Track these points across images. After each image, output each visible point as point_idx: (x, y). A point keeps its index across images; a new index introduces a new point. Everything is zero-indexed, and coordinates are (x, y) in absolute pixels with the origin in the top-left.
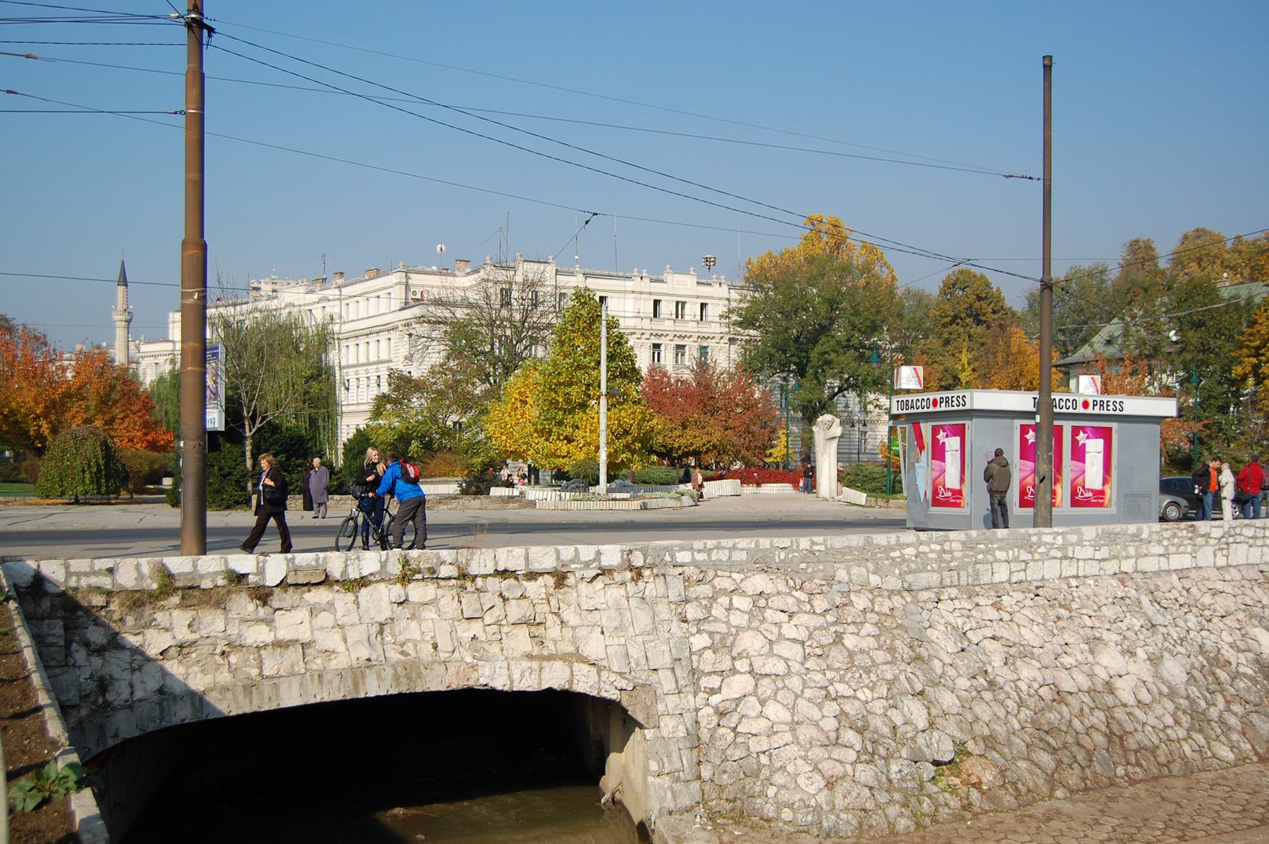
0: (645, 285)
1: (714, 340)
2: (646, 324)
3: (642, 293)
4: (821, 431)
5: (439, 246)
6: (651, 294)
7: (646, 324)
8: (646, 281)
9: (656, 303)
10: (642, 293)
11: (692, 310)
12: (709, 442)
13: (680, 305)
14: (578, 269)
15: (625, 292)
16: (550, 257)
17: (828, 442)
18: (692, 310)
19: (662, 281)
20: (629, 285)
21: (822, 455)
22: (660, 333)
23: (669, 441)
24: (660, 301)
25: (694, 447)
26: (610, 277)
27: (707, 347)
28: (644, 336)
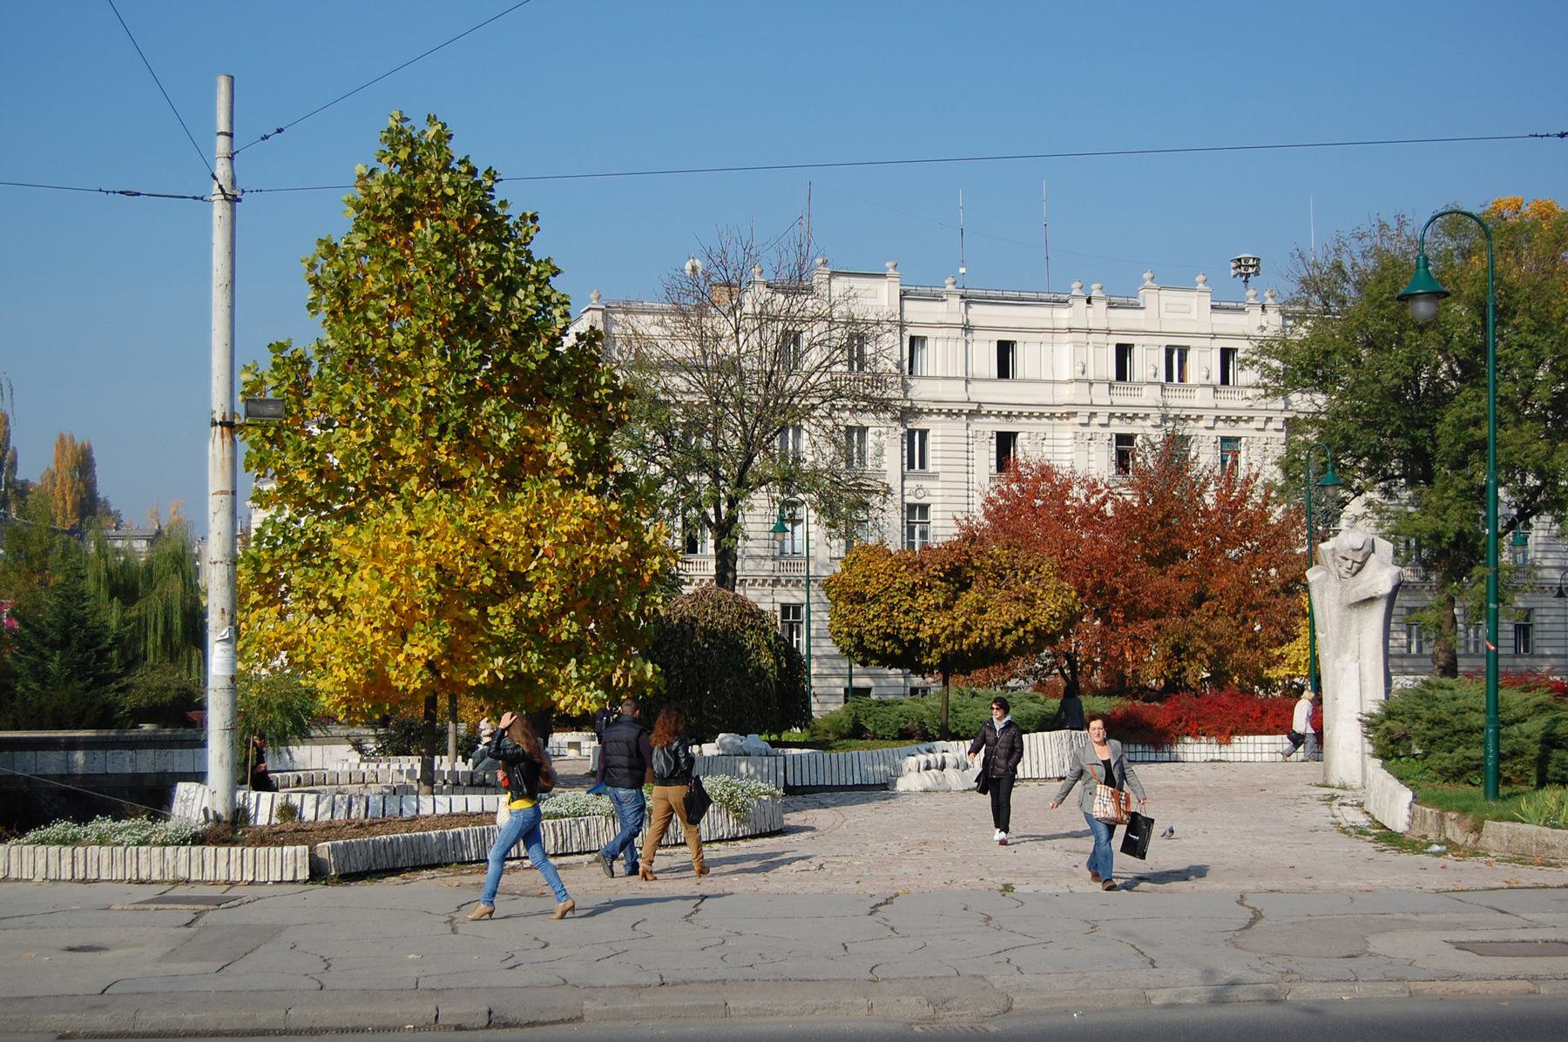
0: (1098, 315)
1: (1253, 425)
2: (1101, 394)
3: (1089, 331)
4: (1333, 583)
5: (688, 266)
6: (1109, 332)
7: (1101, 394)
8: (1100, 306)
9: (1123, 352)
10: (1089, 331)
11: (1203, 364)
12: (1020, 623)
13: (1176, 358)
14: (950, 287)
15: (1054, 331)
16: (888, 265)
17: (1354, 614)
18: (1203, 364)
19: (1136, 307)
20: (1063, 316)
21: (1337, 656)
22: (1130, 412)
23: (905, 622)
24: (1131, 346)
25: (974, 637)
26: (1021, 301)
27: (1238, 439)
28: (1095, 421)
